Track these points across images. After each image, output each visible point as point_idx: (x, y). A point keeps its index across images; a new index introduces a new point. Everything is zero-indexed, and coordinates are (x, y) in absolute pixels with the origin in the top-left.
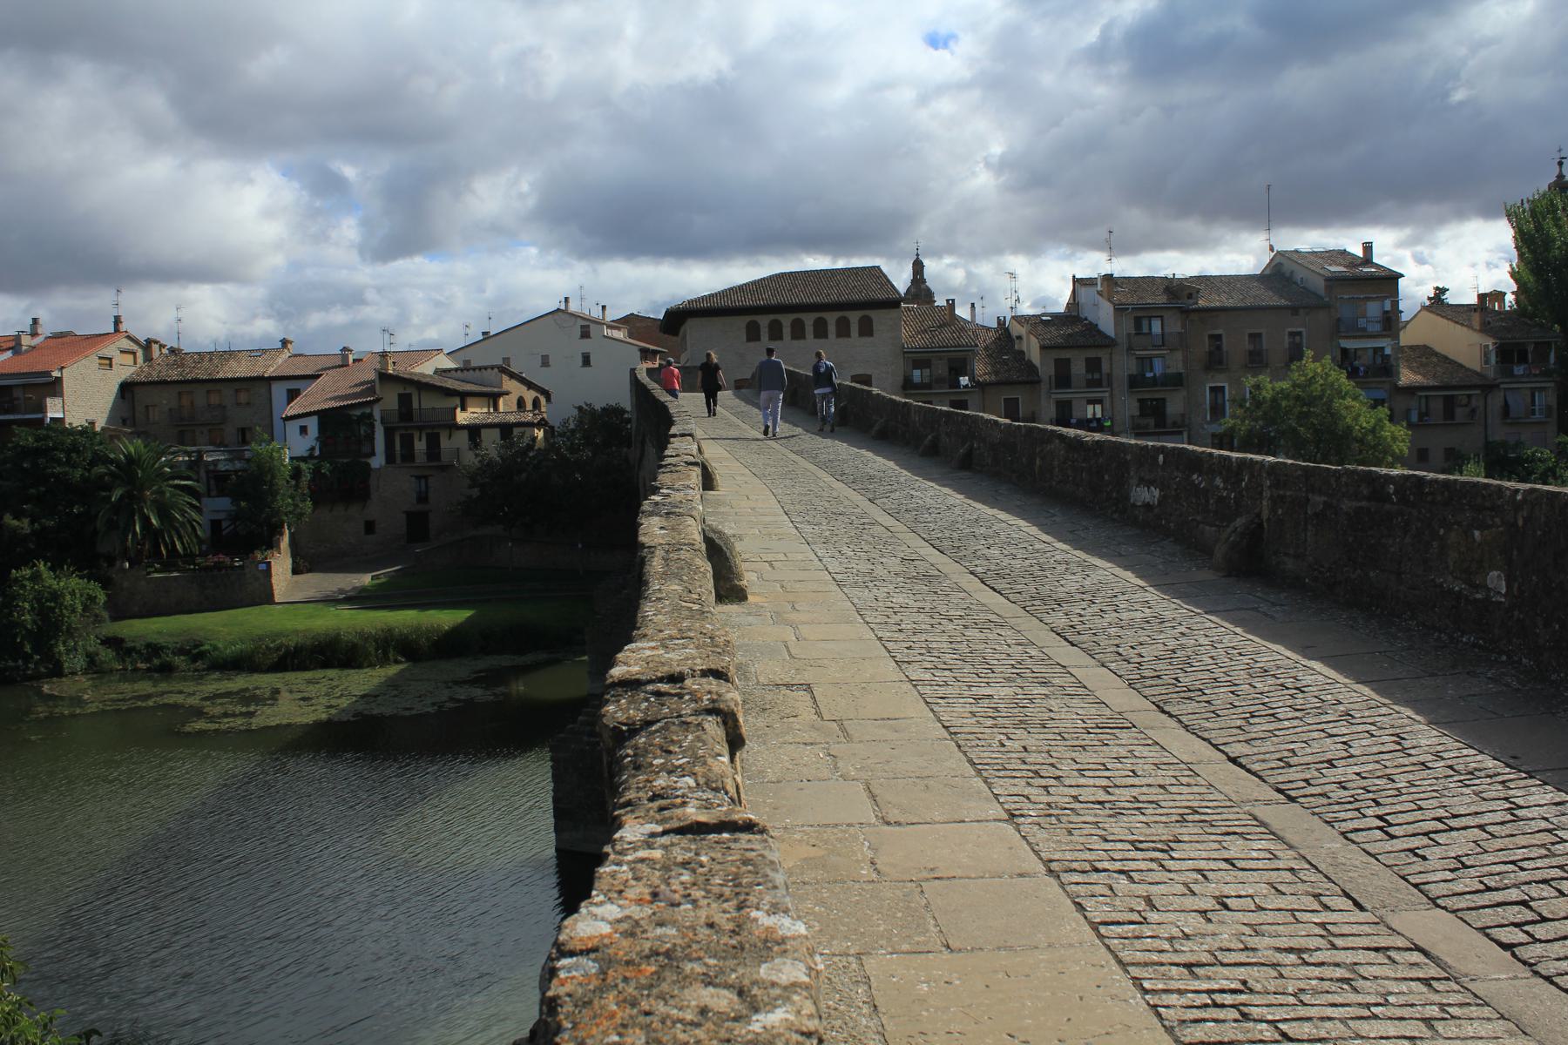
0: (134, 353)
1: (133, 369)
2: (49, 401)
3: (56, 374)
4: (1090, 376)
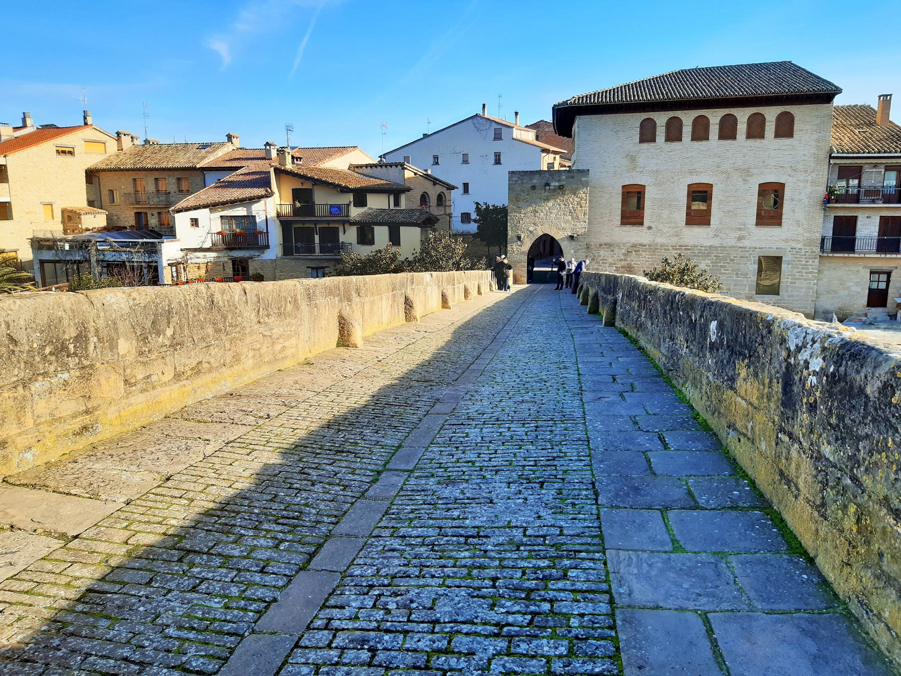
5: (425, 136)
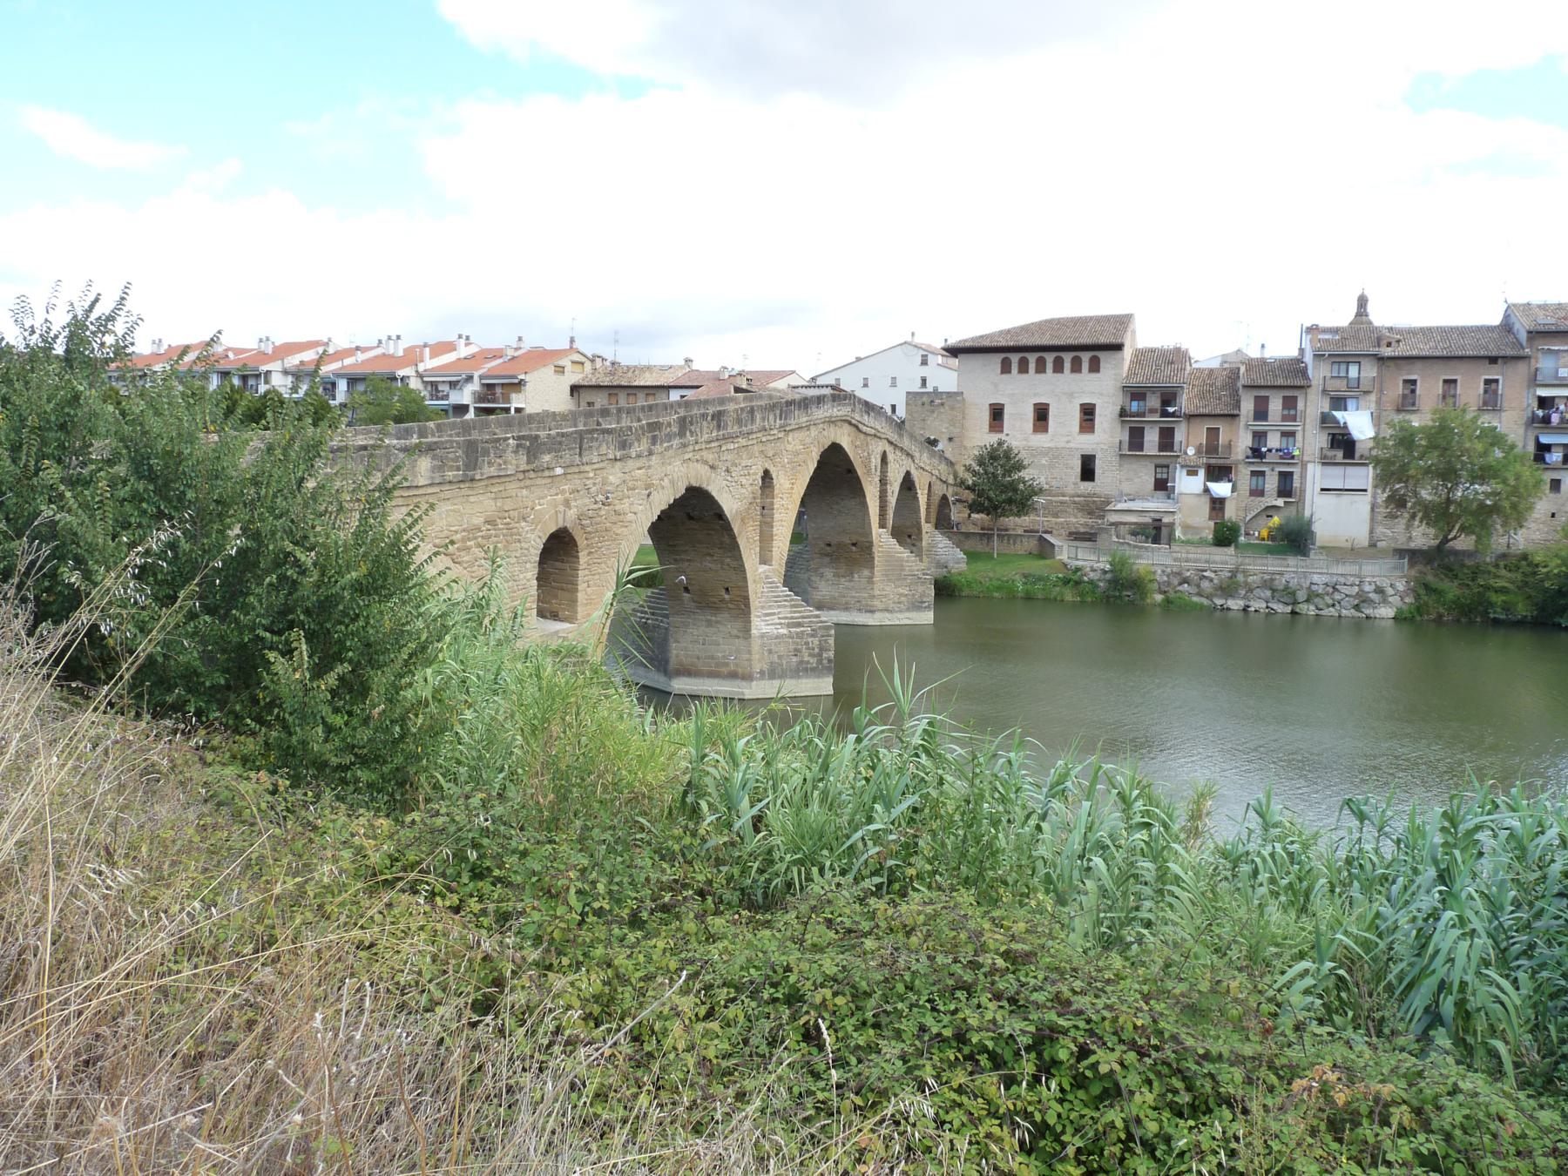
1: (581, 376)
2: (514, 396)
3: (522, 377)
4: (1286, 412)
5: (859, 359)
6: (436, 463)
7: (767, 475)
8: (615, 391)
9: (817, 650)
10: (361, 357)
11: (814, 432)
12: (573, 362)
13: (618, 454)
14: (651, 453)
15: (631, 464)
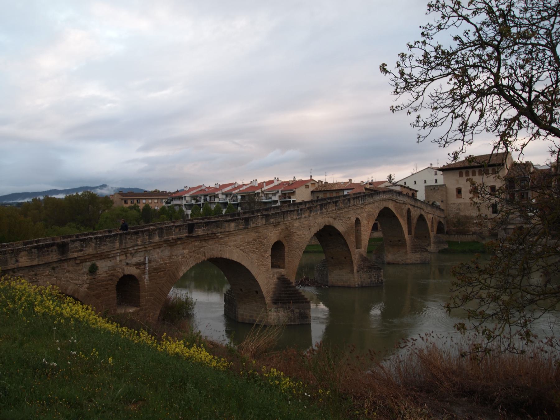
0: (315, 184)
1: (314, 188)
5: (413, 174)
6: (236, 224)
7: (357, 220)
8: (325, 192)
9: (377, 277)
10: (244, 188)
11: (376, 204)
12: (312, 184)
13: (297, 217)
14: (309, 216)
15: (302, 220)
